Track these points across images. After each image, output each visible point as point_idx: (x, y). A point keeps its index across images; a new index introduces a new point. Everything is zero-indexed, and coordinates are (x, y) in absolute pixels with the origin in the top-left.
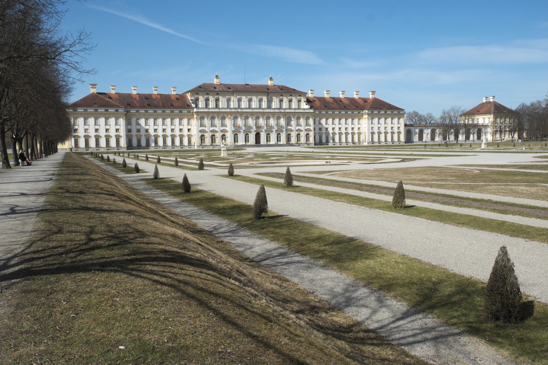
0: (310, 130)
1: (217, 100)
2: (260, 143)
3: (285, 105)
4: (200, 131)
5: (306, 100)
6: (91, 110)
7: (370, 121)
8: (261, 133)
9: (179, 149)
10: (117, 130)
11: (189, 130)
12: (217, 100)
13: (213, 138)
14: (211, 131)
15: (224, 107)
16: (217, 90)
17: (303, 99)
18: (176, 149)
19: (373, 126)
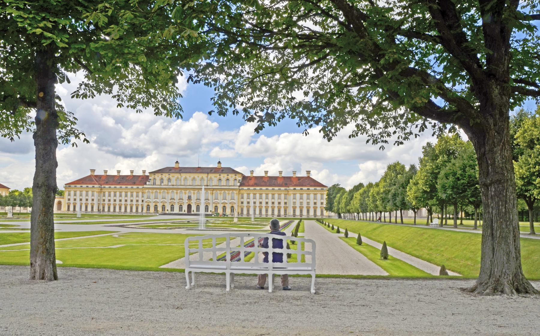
0: (235, 203)
1: (169, 180)
2: (191, 212)
3: (224, 183)
4: (146, 202)
5: (241, 179)
6: (78, 186)
7: (292, 195)
8: (191, 204)
9: (135, 214)
10: (93, 200)
11: (143, 201)
12: (169, 180)
13: (156, 207)
14: (154, 202)
15: (173, 184)
16: (171, 172)
17: (239, 178)
18: (132, 214)
19: (294, 200)
